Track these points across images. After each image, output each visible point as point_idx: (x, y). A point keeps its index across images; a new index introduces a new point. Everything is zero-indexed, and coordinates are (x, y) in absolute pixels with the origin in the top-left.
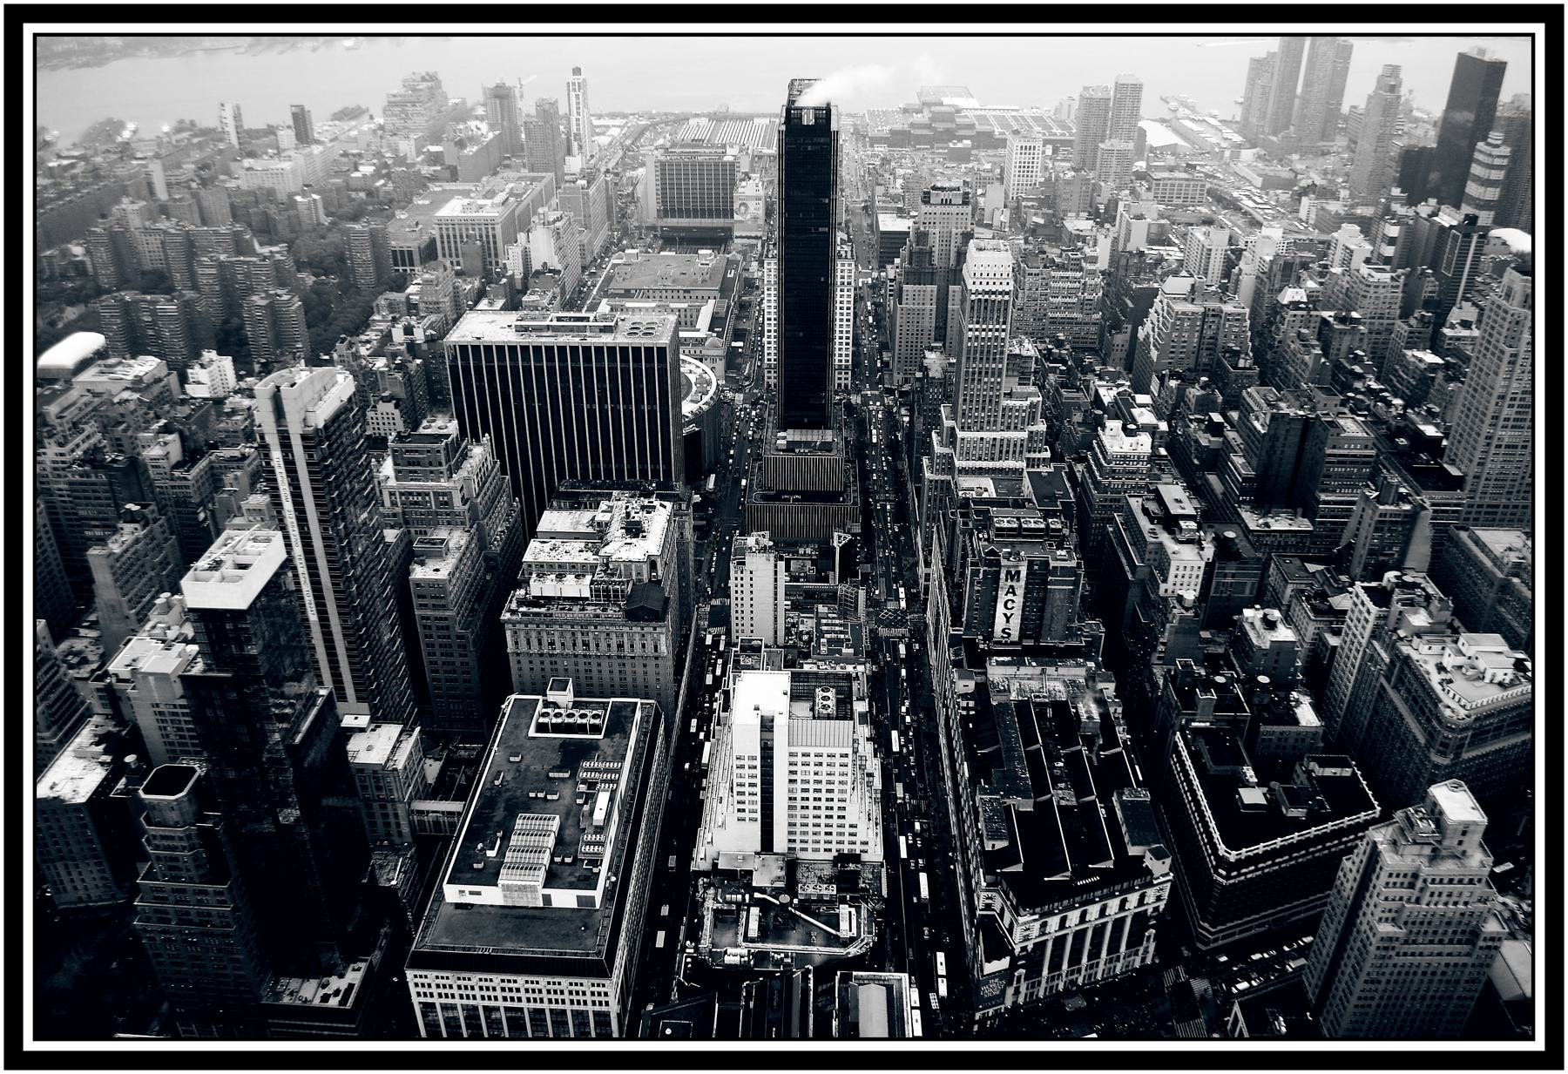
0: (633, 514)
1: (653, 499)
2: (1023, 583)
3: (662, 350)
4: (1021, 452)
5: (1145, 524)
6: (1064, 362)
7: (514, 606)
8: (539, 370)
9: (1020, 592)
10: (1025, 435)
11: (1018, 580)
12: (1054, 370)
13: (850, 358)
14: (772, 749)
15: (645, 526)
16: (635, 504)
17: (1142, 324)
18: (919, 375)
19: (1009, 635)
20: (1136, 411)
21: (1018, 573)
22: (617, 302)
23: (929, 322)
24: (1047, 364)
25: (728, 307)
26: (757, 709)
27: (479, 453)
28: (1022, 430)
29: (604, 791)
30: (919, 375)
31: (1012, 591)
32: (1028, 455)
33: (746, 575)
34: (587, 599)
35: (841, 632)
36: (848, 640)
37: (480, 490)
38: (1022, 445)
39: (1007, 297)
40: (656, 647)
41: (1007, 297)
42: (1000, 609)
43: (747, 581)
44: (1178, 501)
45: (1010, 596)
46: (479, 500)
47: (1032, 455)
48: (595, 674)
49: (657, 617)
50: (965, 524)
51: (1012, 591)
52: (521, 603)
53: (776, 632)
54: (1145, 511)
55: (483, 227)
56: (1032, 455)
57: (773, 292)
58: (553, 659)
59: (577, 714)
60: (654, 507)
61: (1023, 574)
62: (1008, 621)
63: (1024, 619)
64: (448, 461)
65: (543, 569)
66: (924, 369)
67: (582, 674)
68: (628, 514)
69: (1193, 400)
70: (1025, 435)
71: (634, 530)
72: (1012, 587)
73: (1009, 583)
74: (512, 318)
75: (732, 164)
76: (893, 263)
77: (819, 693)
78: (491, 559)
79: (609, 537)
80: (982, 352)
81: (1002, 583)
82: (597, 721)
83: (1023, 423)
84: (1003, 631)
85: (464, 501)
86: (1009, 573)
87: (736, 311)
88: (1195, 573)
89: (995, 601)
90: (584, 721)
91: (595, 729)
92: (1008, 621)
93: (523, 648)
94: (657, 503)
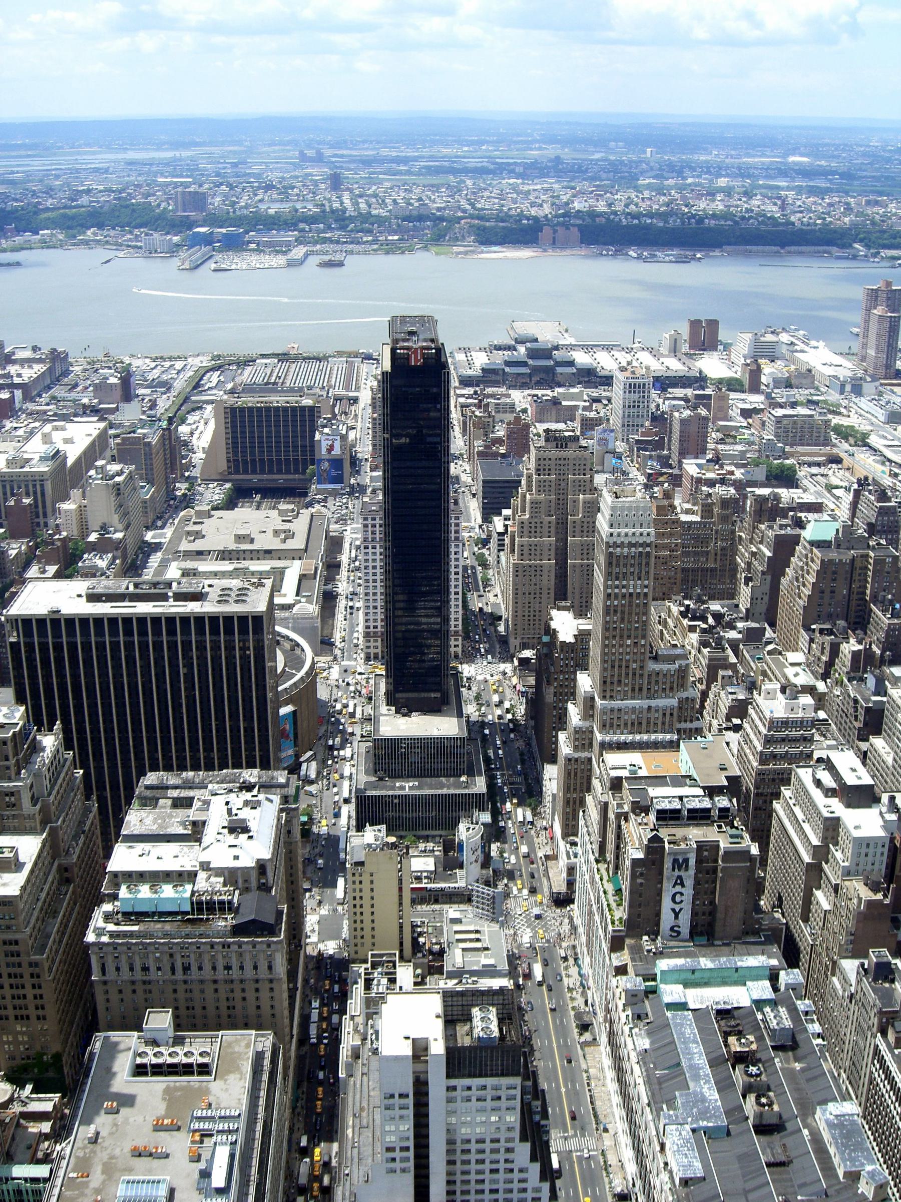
0: (234, 811)
1: (255, 791)
2: (692, 872)
3: (258, 619)
4: (671, 725)
5: (817, 795)
6: (704, 619)
7: (101, 923)
8: (115, 646)
9: (689, 883)
10: (674, 702)
11: (687, 869)
12: (692, 629)
13: (460, 623)
14: (427, 1083)
15: (252, 825)
16: (237, 800)
17: (783, 574)
18: (546, 639)
19: (679, 933)
20: (790, 672)
21: (686, 861)
22: (189, 564)
23: (549, 581)
24: (686, 622)
25: (316, 569)
26: (407, 1038)
27: (49, 742)
28: (673, 697)
29: (222, 1144)
30: (546, 639)
31: (680, 881)
32: (679, 726)
33: (366, 879)
34: (187, 913)
35: (478, 940)
36: (487, 949)
37: (52, 788)
38: (671, 714)
39: (648, 549)
40: (270, 968)
41: (648, 549)
42: (667, 904)
43: (366, 886)
44: (853, 770)
45: (678, 888)
46: (52, 798)
47: (683, 725)
48: (239, 1005)
49: (271, 930)
50: (620, 806)
51: (680, 881)
52: (108, 917)
53: (401, 944)
54: (818, 783)
55: (38, 483)
56: (683, 725)
57: (378, 550)
58: (148, 987)
59: (196, 1052)
60: (259, 803)
61: (692, 862)
62: (676, 917)
63: (694, 914)
64: (16, 754)
65: (135, 878)
66: (553, 634)
67: (182, 1005)
68: (229, 812)
69: (849, 657)
70: (674, 702)
71: (238, 828)
72: (680, 877)
73: (677, 873)
74: (81, 586)
75: (312, 409)
76: (500, 514)
77: (476, 1012)
78: (66, 870)
79: (206, 840)
80: (623, 612)
81: (666, 873)
82: (205, 1060)
83: (672, 688)
84: (672, 929)
85: (34, 800)
86: (675, 861)
87: (325, 573)
88: (879, 850)
89: (660, 894)
90: (190, 1060)
91: (204, 1069)
92: (676, 917)
93: (111, 975)
94: (261, 797)
